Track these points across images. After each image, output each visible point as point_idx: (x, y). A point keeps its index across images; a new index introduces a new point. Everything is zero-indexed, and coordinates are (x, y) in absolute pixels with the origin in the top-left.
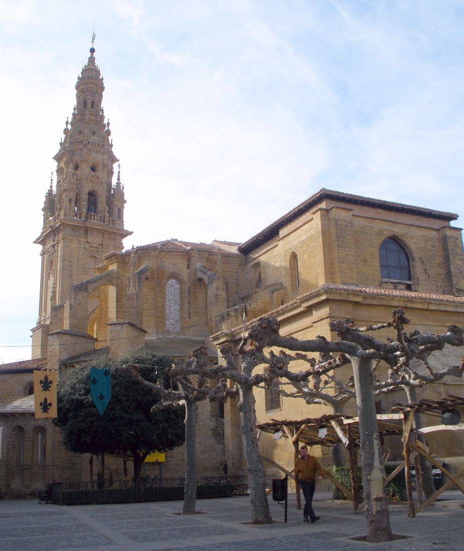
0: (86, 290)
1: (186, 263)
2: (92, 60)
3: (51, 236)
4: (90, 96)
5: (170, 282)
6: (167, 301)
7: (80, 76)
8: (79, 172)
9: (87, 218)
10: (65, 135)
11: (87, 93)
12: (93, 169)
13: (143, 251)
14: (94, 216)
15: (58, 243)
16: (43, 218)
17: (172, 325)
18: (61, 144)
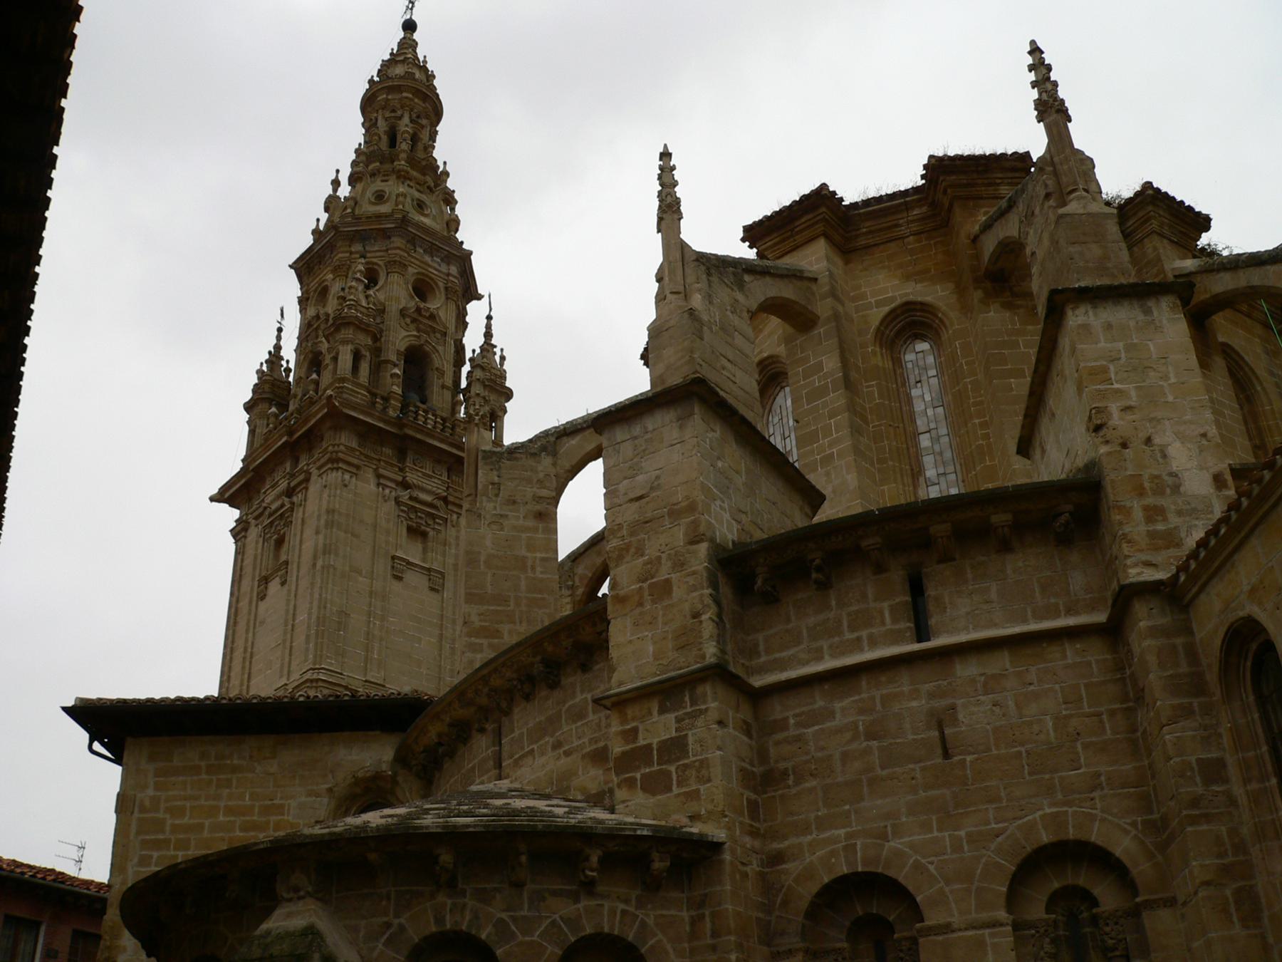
2: (408, 43)
3: (282, 463)
4: (406, 120)
8: (378, 294)
9: (404, 408)
10: (327, 215)
11: (399, 113)
12: (422, 289)
14: (426, 412)
15: (307, 480)
16: (246, 428)
18: (316, 232)
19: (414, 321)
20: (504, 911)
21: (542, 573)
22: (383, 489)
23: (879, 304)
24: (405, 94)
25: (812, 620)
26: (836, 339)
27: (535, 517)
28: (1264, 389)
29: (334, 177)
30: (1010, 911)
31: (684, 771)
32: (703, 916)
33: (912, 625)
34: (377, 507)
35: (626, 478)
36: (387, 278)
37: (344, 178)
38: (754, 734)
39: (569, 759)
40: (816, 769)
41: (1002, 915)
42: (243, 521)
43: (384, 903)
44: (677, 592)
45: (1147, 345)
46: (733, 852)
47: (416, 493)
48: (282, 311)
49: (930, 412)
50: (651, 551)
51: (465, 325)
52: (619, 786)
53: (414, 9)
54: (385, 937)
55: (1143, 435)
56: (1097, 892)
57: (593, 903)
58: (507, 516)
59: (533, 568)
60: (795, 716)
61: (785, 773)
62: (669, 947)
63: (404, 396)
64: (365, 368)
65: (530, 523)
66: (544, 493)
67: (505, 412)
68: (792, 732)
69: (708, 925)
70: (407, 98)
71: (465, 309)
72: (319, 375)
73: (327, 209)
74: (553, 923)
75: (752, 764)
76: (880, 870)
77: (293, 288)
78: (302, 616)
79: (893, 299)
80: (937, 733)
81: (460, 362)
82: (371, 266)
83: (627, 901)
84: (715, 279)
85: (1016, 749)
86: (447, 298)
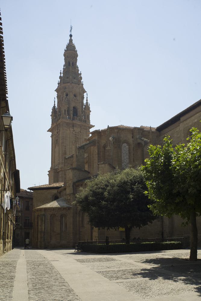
0: (84, 149)
1: (131, 135)
2: (71, 41)
5: (124, 145)
6: (122, 154)
7: (66, 49)
8: (68, 97)
12: (75, 96)
15: (60, 130)
17: (125, 165)
18: (58, 84)
29: (60, 72)
37: (62, 72)
64: (66, 113)
77: (56, 93)
78: (60, 152)
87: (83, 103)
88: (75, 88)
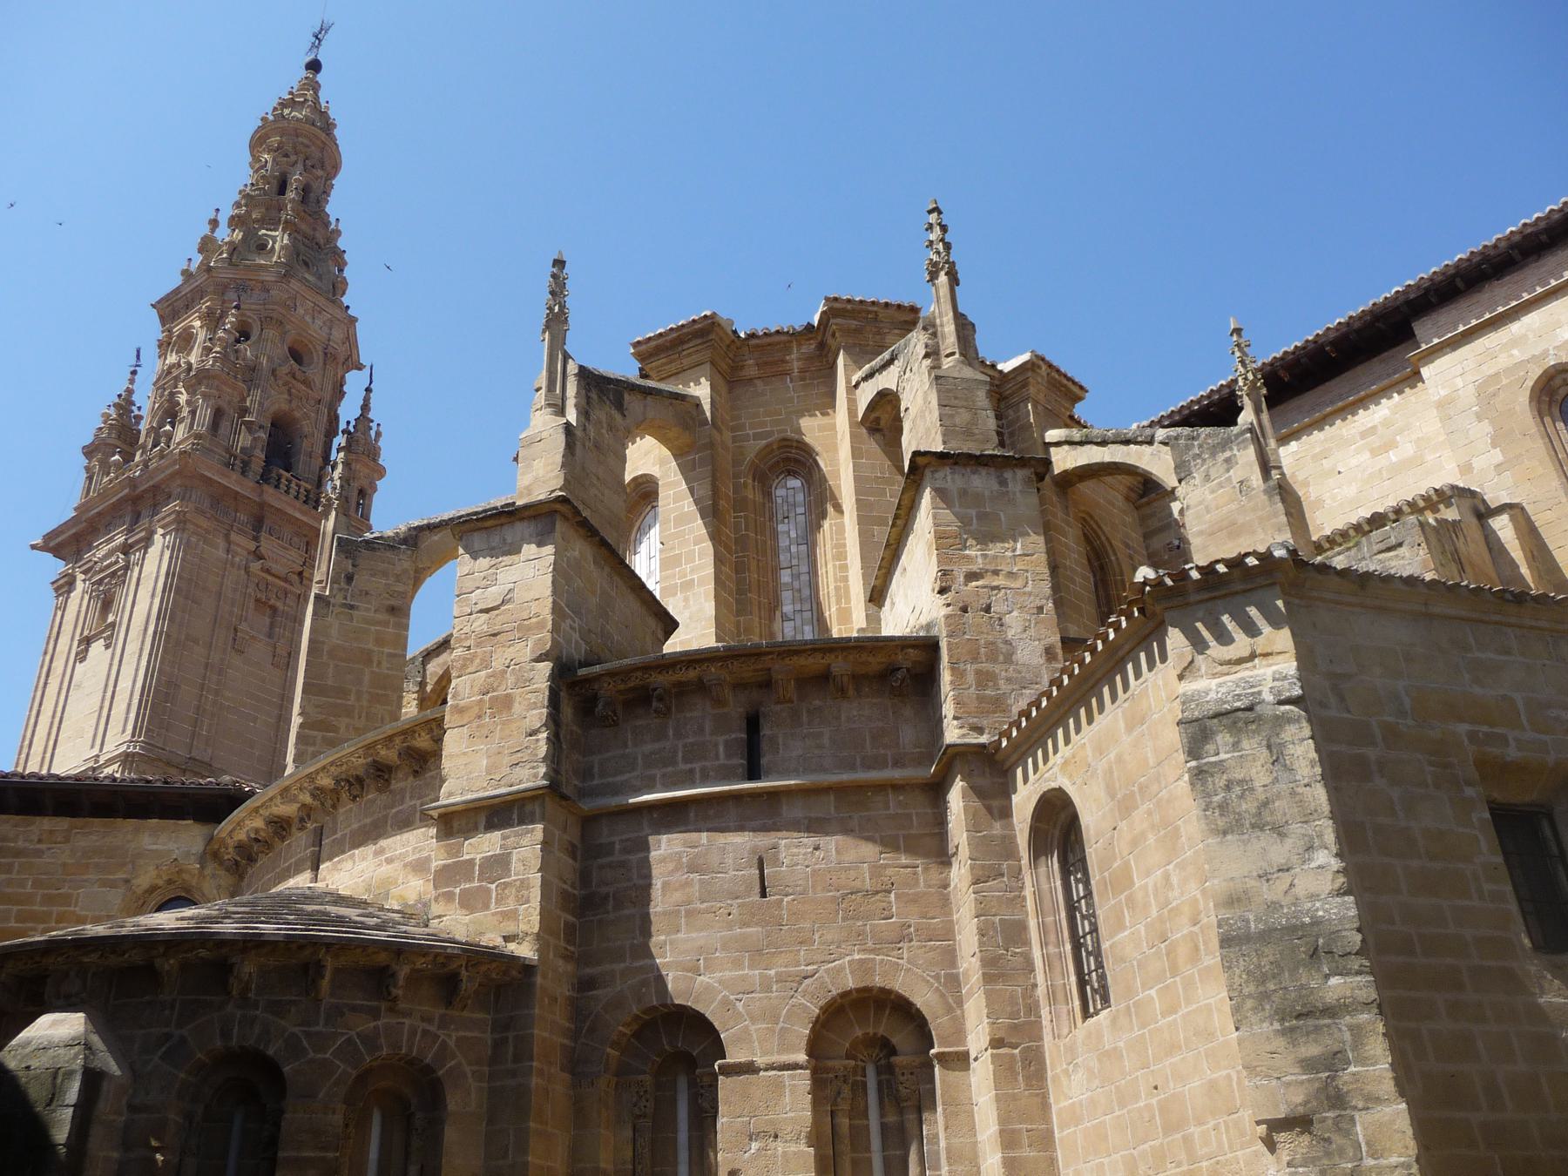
0: (619, 406)
8: (247, 350)
11: (293, 158)
13: (854, 323)
19: (286, 384)
20: (299, 1025)
21: (388, 669)
22: (233, 557)
23: (757, 437)
24: (300, 139)
25: (648, 748)
26: (710, 467)
27: (387, 610)
28: (1117, 559)
30: (811, 1052)
31: (505, 888)
32: (507, 1038)
33: (745, 762)
34: (224, 576)
35: (478, 588)
36: (261, 334)
37: (223, 220)
38: (579, 858)
39: (389, 866)
40: (637, 897)
41: (802, 1057)
42: (69, 574)
43: (167, 1012)
44: (517, 708)
45: (999, 515)
46: (544, 977)
47: (269, 564)
48: (138, 351)
49: (794, 549)
50: (498, 664)
51: (342, 394)
52: (436, 899)
53: (321, 48)
54: (164, 1049)
55: (984, 602)
56: (895, 1040)
57: (393, 1020)
58: (358, 607)
59: (379, 663)
60: (622, 841)
61: (606, 897)
62: (468, 1069)
63: (268, 461)
65: (381, 617)
66: (400, 588)
67: (375, 490)
68: (617, 857)
69: (511, 1049)
70: (302, 143)
71: (343, 377)
72: (173, 428)
73: (200, 251)
74: (349, 1041)
75: (573, 886)
76: (689, 1004)
77: (153, 329)
78: (125, 684)
79: (770, 434)
80: (757, 872)
81: (331, 432)
82: (244, 319)
83: (427, 1019)
84: (594, 395)
85: (831, 894)
86: (325, 364)
87: (337, 418)
88: (301, 311)
